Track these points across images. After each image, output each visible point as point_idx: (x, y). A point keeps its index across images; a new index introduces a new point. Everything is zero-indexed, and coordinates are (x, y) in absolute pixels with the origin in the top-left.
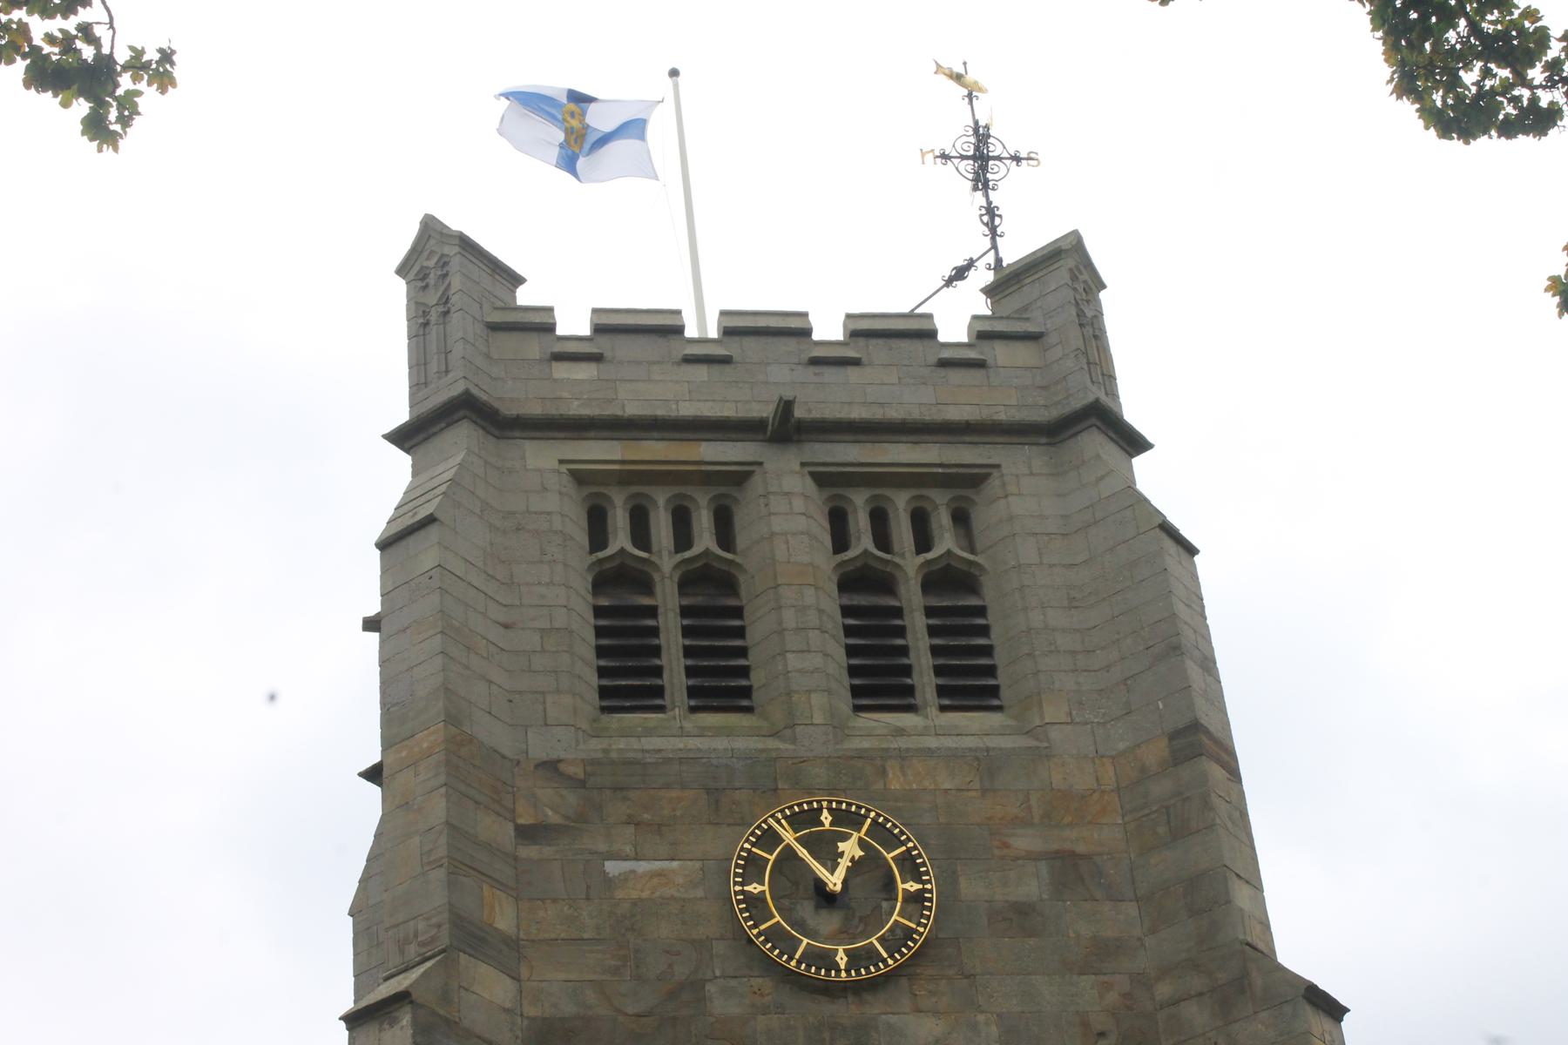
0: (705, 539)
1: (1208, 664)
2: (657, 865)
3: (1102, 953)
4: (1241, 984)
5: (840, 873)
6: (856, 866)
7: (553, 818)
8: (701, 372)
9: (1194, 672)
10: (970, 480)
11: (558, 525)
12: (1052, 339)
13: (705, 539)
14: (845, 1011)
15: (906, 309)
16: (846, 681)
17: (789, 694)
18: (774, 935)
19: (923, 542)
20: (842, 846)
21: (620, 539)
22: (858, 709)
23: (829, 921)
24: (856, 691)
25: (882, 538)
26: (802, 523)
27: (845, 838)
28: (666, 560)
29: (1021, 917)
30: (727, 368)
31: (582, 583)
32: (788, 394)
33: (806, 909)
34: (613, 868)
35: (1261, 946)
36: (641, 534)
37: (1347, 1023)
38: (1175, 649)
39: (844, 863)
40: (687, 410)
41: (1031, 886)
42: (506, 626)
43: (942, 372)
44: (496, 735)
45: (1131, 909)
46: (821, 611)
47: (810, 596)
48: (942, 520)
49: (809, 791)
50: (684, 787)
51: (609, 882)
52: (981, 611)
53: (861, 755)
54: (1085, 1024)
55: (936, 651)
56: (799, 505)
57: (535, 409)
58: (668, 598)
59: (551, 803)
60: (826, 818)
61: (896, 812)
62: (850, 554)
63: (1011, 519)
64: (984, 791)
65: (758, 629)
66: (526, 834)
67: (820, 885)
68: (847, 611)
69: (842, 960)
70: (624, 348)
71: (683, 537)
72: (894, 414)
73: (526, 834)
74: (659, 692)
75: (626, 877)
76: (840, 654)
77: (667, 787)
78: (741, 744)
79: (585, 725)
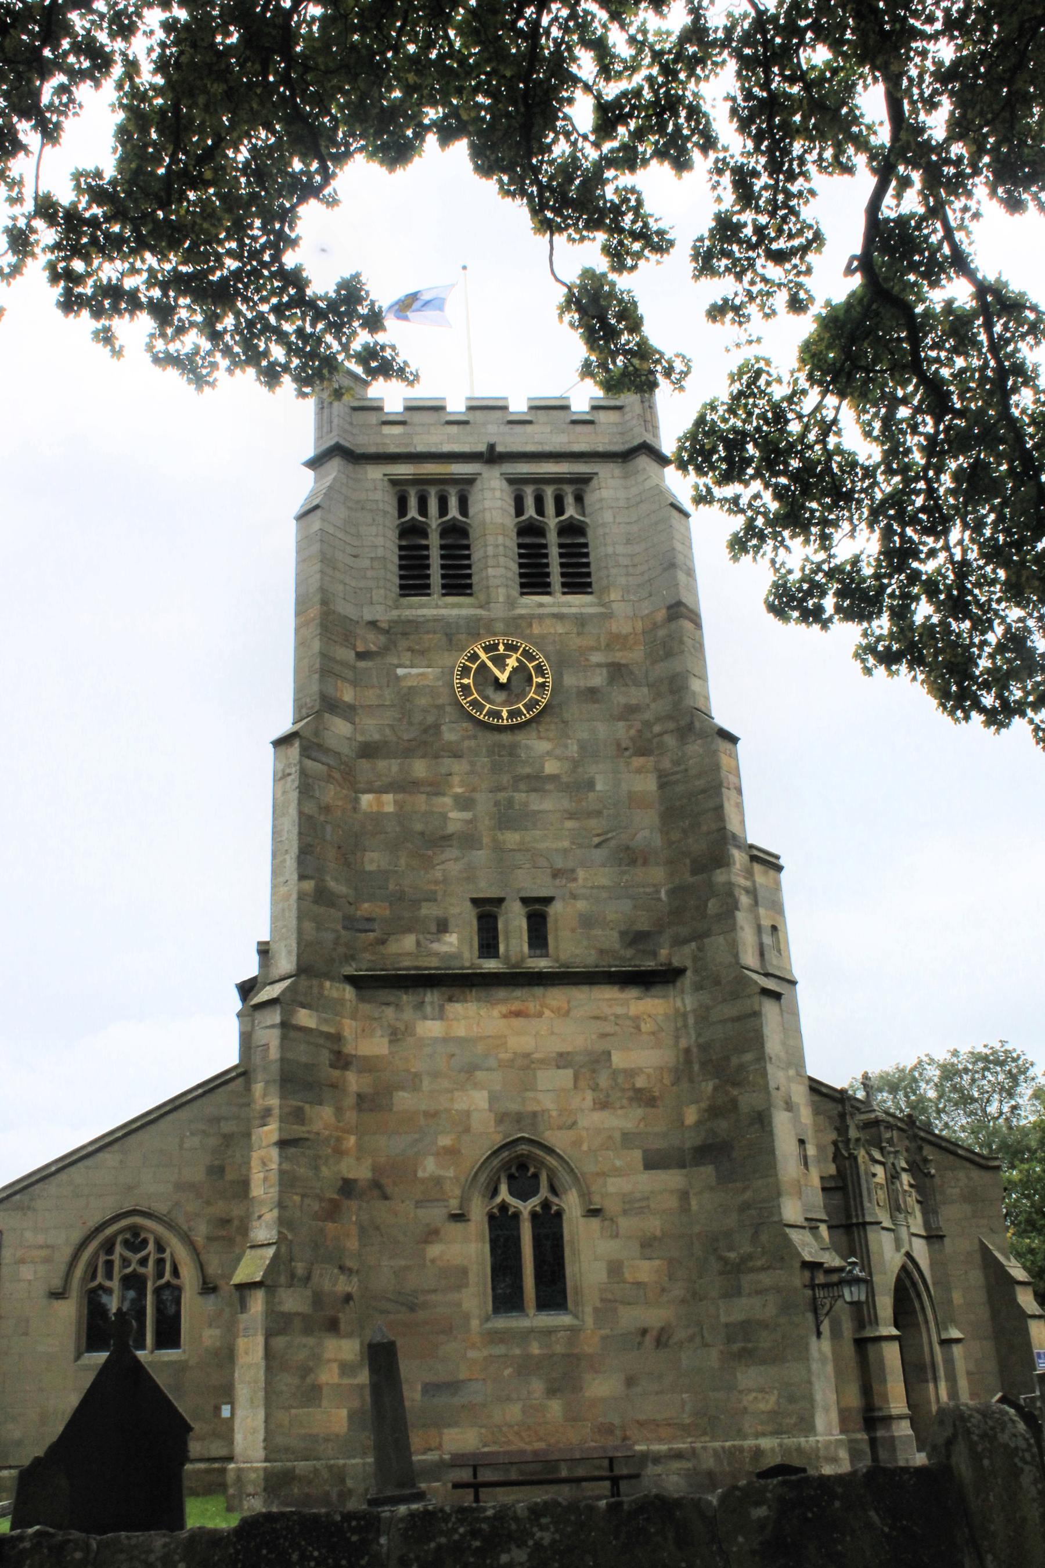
0: (454, 512)
1: (690, 573)
2: (421, 670)
3: (630, 711)
4: (690, 727)
5: (507, 674)
6: (515, 670)
7: (373, 648)
8: (454, 429)
9: (681, 576)
10: (582, 481)
11: (381, 505)
12: (627, 409)
13: (454, 512)
14: (506, 738)
15: (558, 395)
16: (518, 580)
17: (488, 587)
18: (475, 703)
19: (560, 510)
20: (508, 661)
21: (413, 513)
22: (522, 594)
23: (500, 697)
24: (522, 585)
25: (540, 510)
26: (499, 503)
27: (509, 657)
28: (434, 522)
29: (591, 694)
30: (468, 427)
31: (393, 535)
32: (492, 441)
33: (490, 692)
34: (400, 671)
35: (703, 709)
36: (423, 510)
37: (740, 744)
38: (672, 565)
39: (509, 669)
40: (446, 448)
41: (598, 679)
42: (355, 556)
43: (571, 426)
44: (345, 608)
45: (645, 690)
46: (505, 547)
47: (500, 539)
48: (569, 500)
49: (495, 634)
50: (435, 632)
51: (398, 678)
52: (586, 545)
53: (521, 617)
54: (618, 745)
55: (562, 565)
56: (498, 494)
57: (372, 450)
58: (434, 541)
59: (371, 641)
60: (501, 647)
61: (535, 644)
62: (523, 518)
63: (601, 500)
64: (579, 634)
65: (476, 555)
66: (361, 656)
67: (497, 679)
68: (520, 546)
69: (505, 714)
70: (417, 417)
71: (443, 510)
72: (547, 448)
73: (361, 656)
74: (428, 586)
75: (406, 676)
76: (515, 567)
77: (428, 632)
78: (464, 612)
79: (390, 603)
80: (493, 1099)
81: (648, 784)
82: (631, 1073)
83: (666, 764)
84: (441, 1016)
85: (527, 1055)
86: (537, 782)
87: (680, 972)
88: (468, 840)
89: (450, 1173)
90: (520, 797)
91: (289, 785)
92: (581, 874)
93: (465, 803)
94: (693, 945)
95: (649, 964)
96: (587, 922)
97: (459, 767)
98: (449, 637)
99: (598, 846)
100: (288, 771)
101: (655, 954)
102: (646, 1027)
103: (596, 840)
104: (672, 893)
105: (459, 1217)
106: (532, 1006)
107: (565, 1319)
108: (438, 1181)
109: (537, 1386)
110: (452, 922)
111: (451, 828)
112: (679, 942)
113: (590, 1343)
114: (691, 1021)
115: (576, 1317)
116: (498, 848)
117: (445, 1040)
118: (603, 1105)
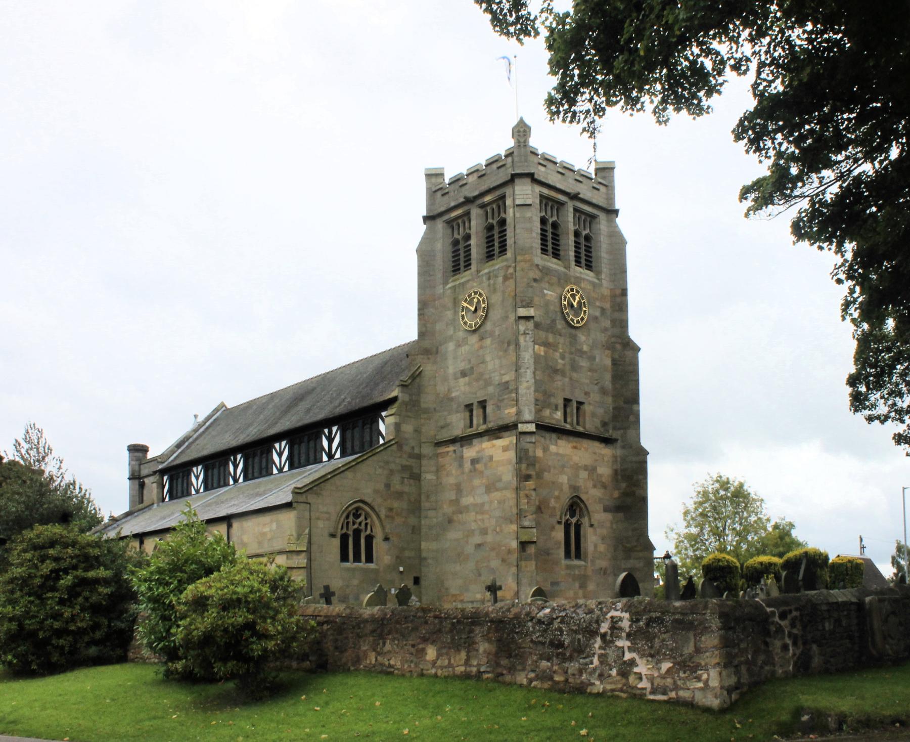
8: (560, 176)
14: (573, 331)
29: (596, 318)
34: (546, 292)
40: (558, 186)
51: (545, 295)
75: (547, 294)
80: (568, 480)
81: (608, 362)
82: (601, 476)
83: (616, 356)
84: (556, 445)
85: (577, 464)
86: (581, 353)
87: (616, 440)
88: (563, 374)
89: (557, 506)
90: (577, 358)
91: (528, 338)
92: (592, 395)
93: (563, 358)
94: (622, 431)
95: (606, 435)
96: (593, 415)
97: (561, 340)
98: (559, 279)
99: (596, 384)
100: (527, 332)
101: (608, 431)
102: (606, 459)
103: (596, 382)
104: (614, 409)
105: (559, 523)
106: (578, 445)
107: (582, 563)
108: (554, 508)
109: (577, 585)
110: (559, 407)
111: (559, 367)
112: (615, 428)
113: (589, 573)
114: (619, 459)
115: (585, 561)
116: (571, 379)
117: (557, 454)
118: (595, 486)
